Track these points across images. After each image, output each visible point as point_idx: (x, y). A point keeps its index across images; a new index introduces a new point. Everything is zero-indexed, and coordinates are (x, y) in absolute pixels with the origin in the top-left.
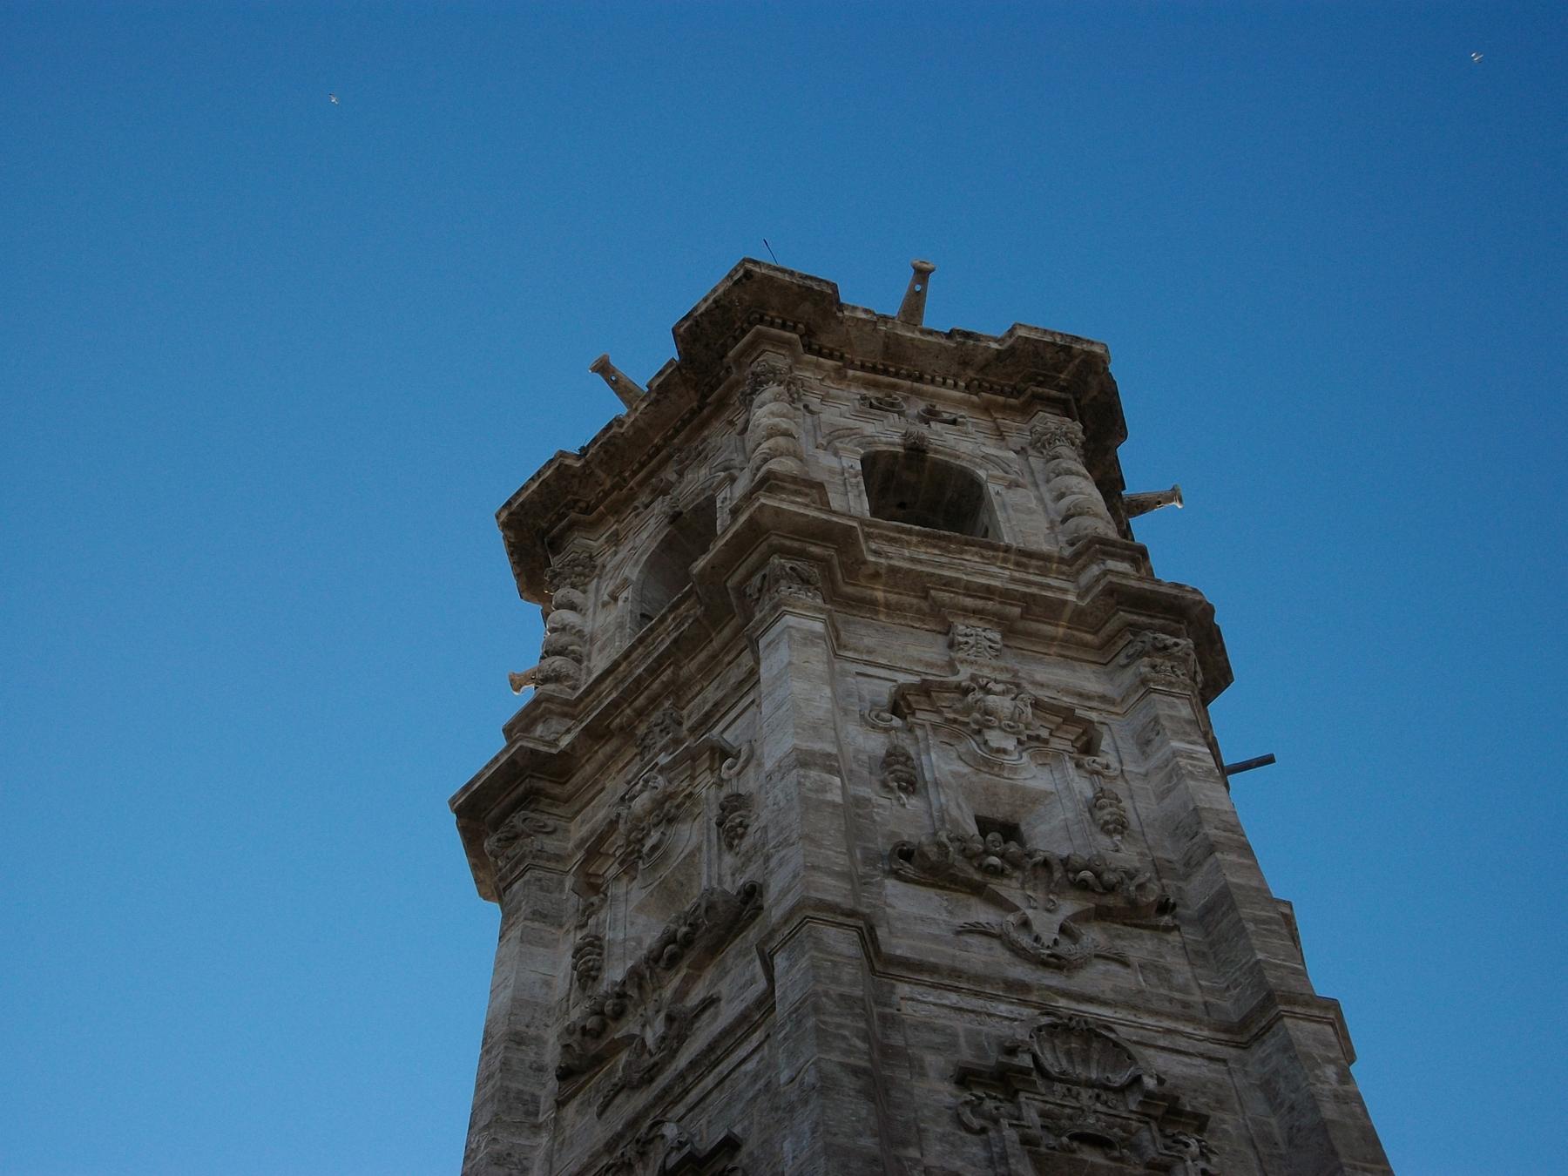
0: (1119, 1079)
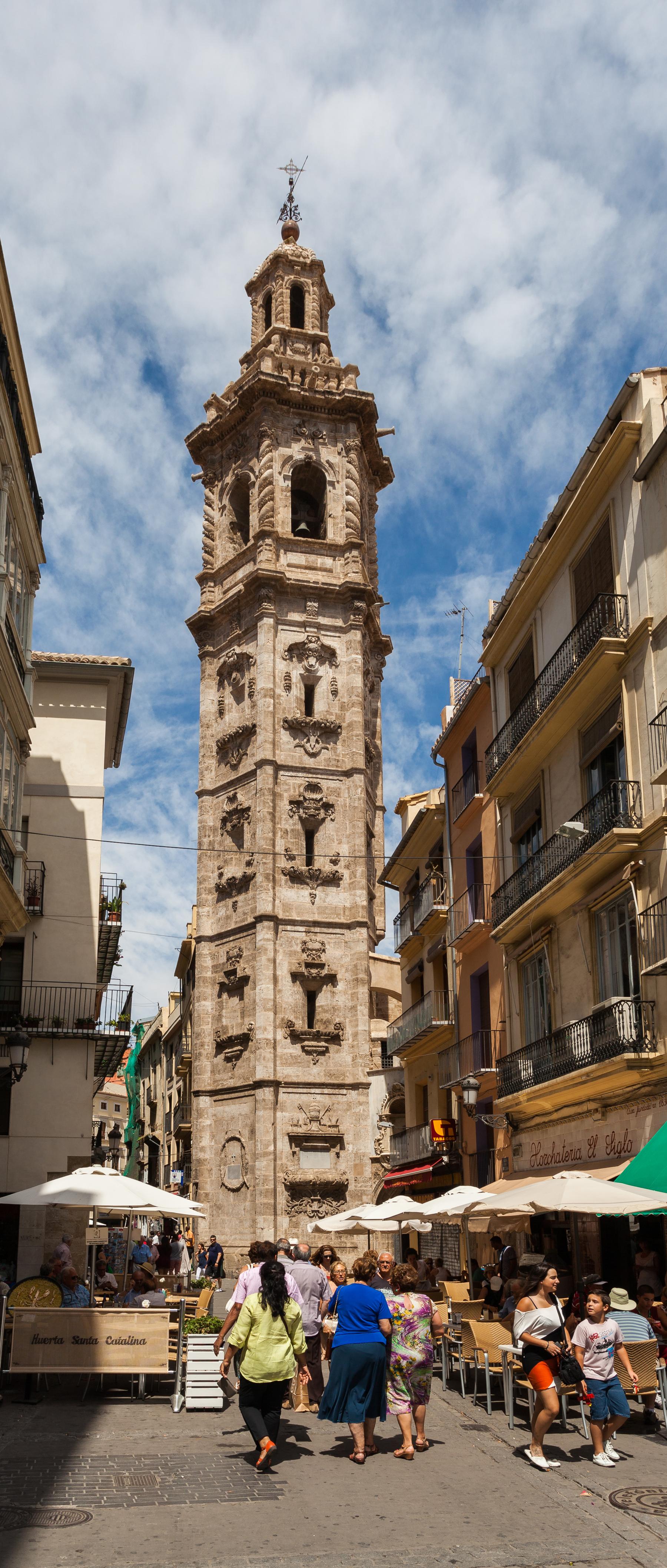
0: (317, 796)
